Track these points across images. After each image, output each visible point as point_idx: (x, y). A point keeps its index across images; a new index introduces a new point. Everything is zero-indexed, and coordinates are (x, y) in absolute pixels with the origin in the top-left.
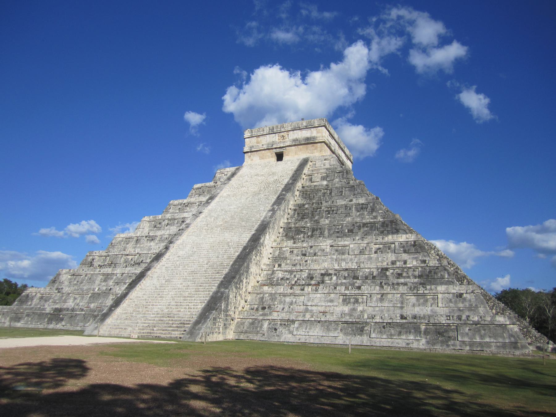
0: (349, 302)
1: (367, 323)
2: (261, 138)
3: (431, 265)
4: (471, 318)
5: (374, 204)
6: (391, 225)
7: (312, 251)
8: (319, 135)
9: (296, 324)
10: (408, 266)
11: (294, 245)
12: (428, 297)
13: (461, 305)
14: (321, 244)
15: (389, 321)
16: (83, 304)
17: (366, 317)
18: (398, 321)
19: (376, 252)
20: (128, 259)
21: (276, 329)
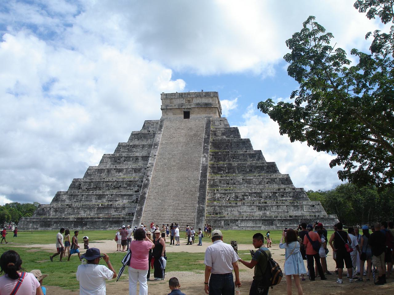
0: (262, 210)
1: (274, 220)
2: (173, 100)
3: (298, 191)
4: (320, 216)
5: (259, 155)
6: (272, 168)
7: (232, 182)
8: (213, 102)
9: (239, 222)
10: (286, 191)
11: (222, 178)
12: (299, 207)
13: (314, 210)
14: (237, 178)
15: (285, 218)
16: (92, 214)
17: (273, 217)
18: (289, 218)
19: (267, 183)
20: (109, 184)
21: (229, 224)
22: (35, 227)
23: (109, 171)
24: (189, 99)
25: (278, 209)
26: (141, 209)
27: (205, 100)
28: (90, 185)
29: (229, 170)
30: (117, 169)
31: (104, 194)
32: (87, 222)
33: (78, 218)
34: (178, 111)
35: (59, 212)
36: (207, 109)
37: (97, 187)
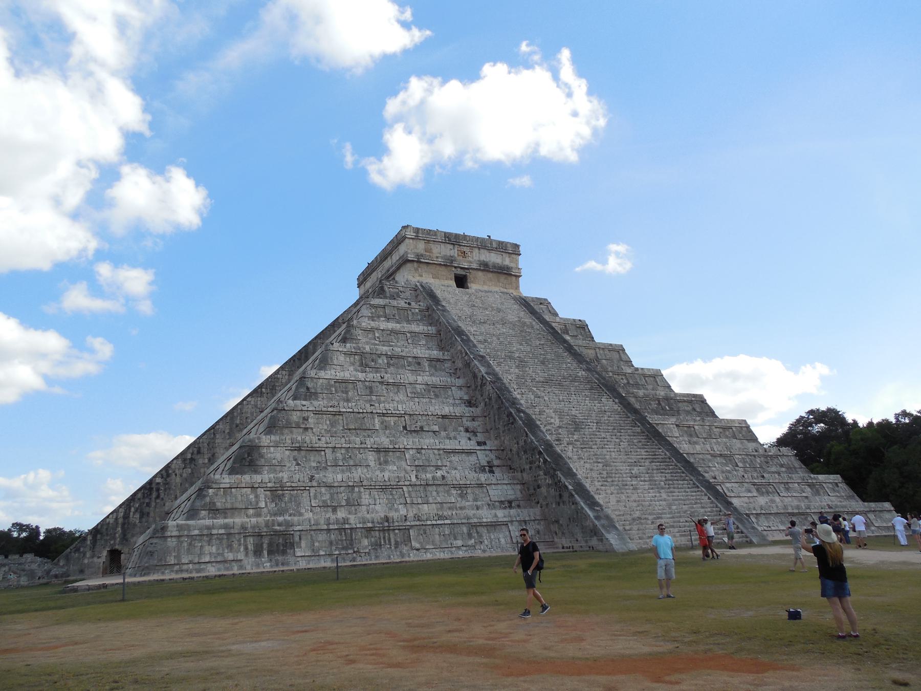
2: (432, 246)
8: (512, 265)
22: (230, 556)
24: (465, 249)
25: (788, 489)
27: (494, 258)
31: (397, 446)
34: (443, 271)
36: (502, 278)
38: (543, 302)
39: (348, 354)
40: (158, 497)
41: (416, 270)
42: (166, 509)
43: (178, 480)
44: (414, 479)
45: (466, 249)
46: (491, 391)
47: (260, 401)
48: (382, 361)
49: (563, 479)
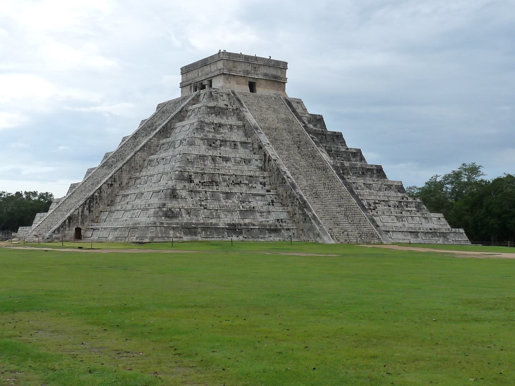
1: (418, 232)
2: (236, 64)
8: (282, 76)
16: (236, 219)
20: (226, 179)
23: (214, 159)
26: (314, 215)
27: (272, 72)
28: (203, 178)
29: (343, 171)
30: (223, 157)
32: (241, 229)
33: (229, 224)
34: (243, 80)
35: (193, 215)
37: (213, 182)
38: (299, 102)
39: (202, 139)
40: (97, 203)
41: (227, 79)
42: (100, 209)
43: (105, 195)
44: (241, 207)
45: (257, 67)
46: (274, 165)
47: (144, 154)
48: (218, 143)
49: (307, 213)
